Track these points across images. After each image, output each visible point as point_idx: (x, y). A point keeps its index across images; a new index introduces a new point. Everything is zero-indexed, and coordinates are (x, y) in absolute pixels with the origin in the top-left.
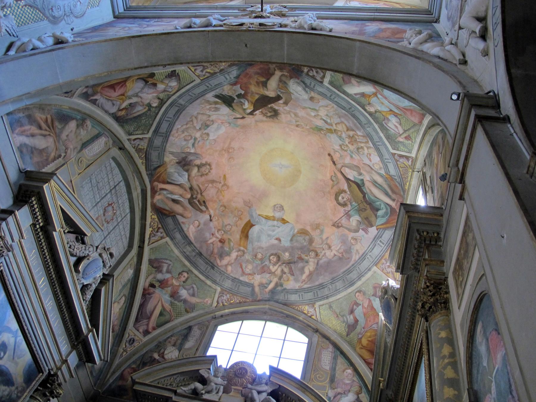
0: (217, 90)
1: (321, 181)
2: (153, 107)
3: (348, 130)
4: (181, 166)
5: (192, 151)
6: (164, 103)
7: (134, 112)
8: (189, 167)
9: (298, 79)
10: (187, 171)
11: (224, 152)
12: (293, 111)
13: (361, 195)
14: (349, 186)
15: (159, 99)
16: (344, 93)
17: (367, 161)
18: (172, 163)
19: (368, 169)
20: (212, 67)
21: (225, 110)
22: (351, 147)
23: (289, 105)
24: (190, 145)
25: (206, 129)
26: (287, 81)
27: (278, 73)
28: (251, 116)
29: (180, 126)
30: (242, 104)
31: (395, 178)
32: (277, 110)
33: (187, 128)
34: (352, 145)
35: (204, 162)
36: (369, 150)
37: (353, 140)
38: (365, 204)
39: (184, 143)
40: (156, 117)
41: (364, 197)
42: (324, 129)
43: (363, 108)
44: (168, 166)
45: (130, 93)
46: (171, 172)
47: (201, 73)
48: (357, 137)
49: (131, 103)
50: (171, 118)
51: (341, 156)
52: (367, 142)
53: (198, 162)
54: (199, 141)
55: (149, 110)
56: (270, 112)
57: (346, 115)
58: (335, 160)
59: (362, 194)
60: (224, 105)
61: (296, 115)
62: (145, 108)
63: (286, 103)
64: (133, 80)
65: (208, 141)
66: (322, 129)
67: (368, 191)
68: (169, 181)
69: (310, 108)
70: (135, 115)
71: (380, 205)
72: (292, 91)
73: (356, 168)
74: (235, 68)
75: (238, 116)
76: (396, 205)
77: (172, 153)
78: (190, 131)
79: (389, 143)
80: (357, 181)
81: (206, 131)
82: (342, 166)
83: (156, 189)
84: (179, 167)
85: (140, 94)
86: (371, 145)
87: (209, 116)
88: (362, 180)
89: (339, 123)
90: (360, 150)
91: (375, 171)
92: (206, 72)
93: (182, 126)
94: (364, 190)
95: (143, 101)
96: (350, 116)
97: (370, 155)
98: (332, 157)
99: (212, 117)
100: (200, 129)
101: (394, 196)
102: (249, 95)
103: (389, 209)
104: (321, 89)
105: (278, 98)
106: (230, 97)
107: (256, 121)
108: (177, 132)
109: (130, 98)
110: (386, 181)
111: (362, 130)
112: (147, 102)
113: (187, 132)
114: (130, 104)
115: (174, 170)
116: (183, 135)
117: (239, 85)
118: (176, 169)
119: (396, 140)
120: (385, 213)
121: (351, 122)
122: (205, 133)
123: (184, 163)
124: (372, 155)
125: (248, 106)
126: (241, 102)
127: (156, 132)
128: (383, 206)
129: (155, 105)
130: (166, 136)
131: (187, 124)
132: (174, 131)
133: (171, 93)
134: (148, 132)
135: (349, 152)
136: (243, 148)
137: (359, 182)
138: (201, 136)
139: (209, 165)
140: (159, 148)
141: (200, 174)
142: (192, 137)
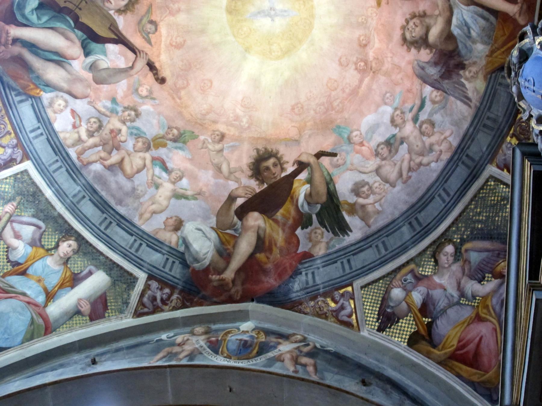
0: (338, 247)
1: (179, 10)
2: (454, 244)
3: (120, 164)
4: (459, 55)
5: (428, 89)
6: (434, 242)
7: (484, 255)
8: (443, 47)
9: (194, 270)
10: (449, 37)
11: (374, 65)
12: (221, 181)
13: (84, 19)
14: (113, 27)
15: (436, 262)
16: (110, 267)
17: (80, 106)
18: (474, 69)
19: (78, 89)
20: (325, 310)
21: (343, 187)
22: (115, 123)
23: (226, 195)
24: (428, 106)
25: (394, 136)
26: (217, 258)
27: (229, 275)
28: (304, 159)
29: (433, 165)
30: (309, 197)
31: (18, 98)
32: (252, 176)
33: (422, 154)
34: (112, 131)
35: (413, 50)
36: (76, 136)
37: (112, 144)
38: (70, 6)
39: (437, 118)
40: (460, 215)
41: (76, 19)
42: (170, 144)
43: (83, 238)
44: (484, 62)
45: (467, 313)
46: (484, 43)
47: (346, 303)
48: (103, 154)
49: (480, 282)
50: (439, 195)
51: (137, 90)
52: (80, 154)
53: (425, 55)
54: (411, 110)
55: (463, 241)
56: (268, 168)
57: (120, 202)
58: (150, 75)
59: (83, 24)
60: (341, 199)
61: (218, 169)
62: (466, 251)
63: (231, 199)
64: (443, 348)
65: (395, 105)
66: (175, 140)
67: (72, 36)
68: (492, 18)
69: (186, 197)
70: (486, 244)
71: (39, 18)
72: (213, 235)
73: (101, 77)
74: (294, 295)
75: (325, 161)
76: (7, 33)
77: (466, 100)
78: (419, 144)
79: (34, 183)
80: (99, 46)
81: (395, 131)
82: (132, 68)
83: (525, 7)
84: (463, 52)
85: (455, 294)
86: (73, 153)
87: (377, 171)
88: (87, 54)
89: (139, 171)
90: (95, 126)
91: (60, 90)
92: (336, 302)
93: (428, 164)
94: (80, 33)
95: (460, 275)
96: (112, 202)
97: (74, 127)
98: (157, 79)
99: (374, 167)
100: (402, 141)
101: (17, 49)
102: (290, 222)
103: (19, 18)
104: (155, 258)
105: (242, 212)
106: (322, 224)
107: (297, 142)
108: (441, 151)
109: (474, 297)
110: (38, 77)
111: (90, 178)
112: (456, 267)
113: (423, 142)
114: (480, 281)
115: (474, 46)
116: (433, 139)
117: (300, 250)
118: (471, 51)
119: (18, 198)
120: (24, 7)
121: (113, 186)
122: (396, 126)
123: (449, 60)
124: (70, 127)
125: (301, 190)
126: (309, 204)
127: (473, 176)
128: (34, 18)
129: (449, 249)
130: (460, 153)
131: (420, 164)
132: (445, 157)
133: (412, 266)
134: (487, 181)
135: (120, 109)
136: (341, 64)
137: (94, 46)
138: (404, 122)
139: (404, 39)
140: (485, 126)
141: (427, 20)
142: (421, 127)
